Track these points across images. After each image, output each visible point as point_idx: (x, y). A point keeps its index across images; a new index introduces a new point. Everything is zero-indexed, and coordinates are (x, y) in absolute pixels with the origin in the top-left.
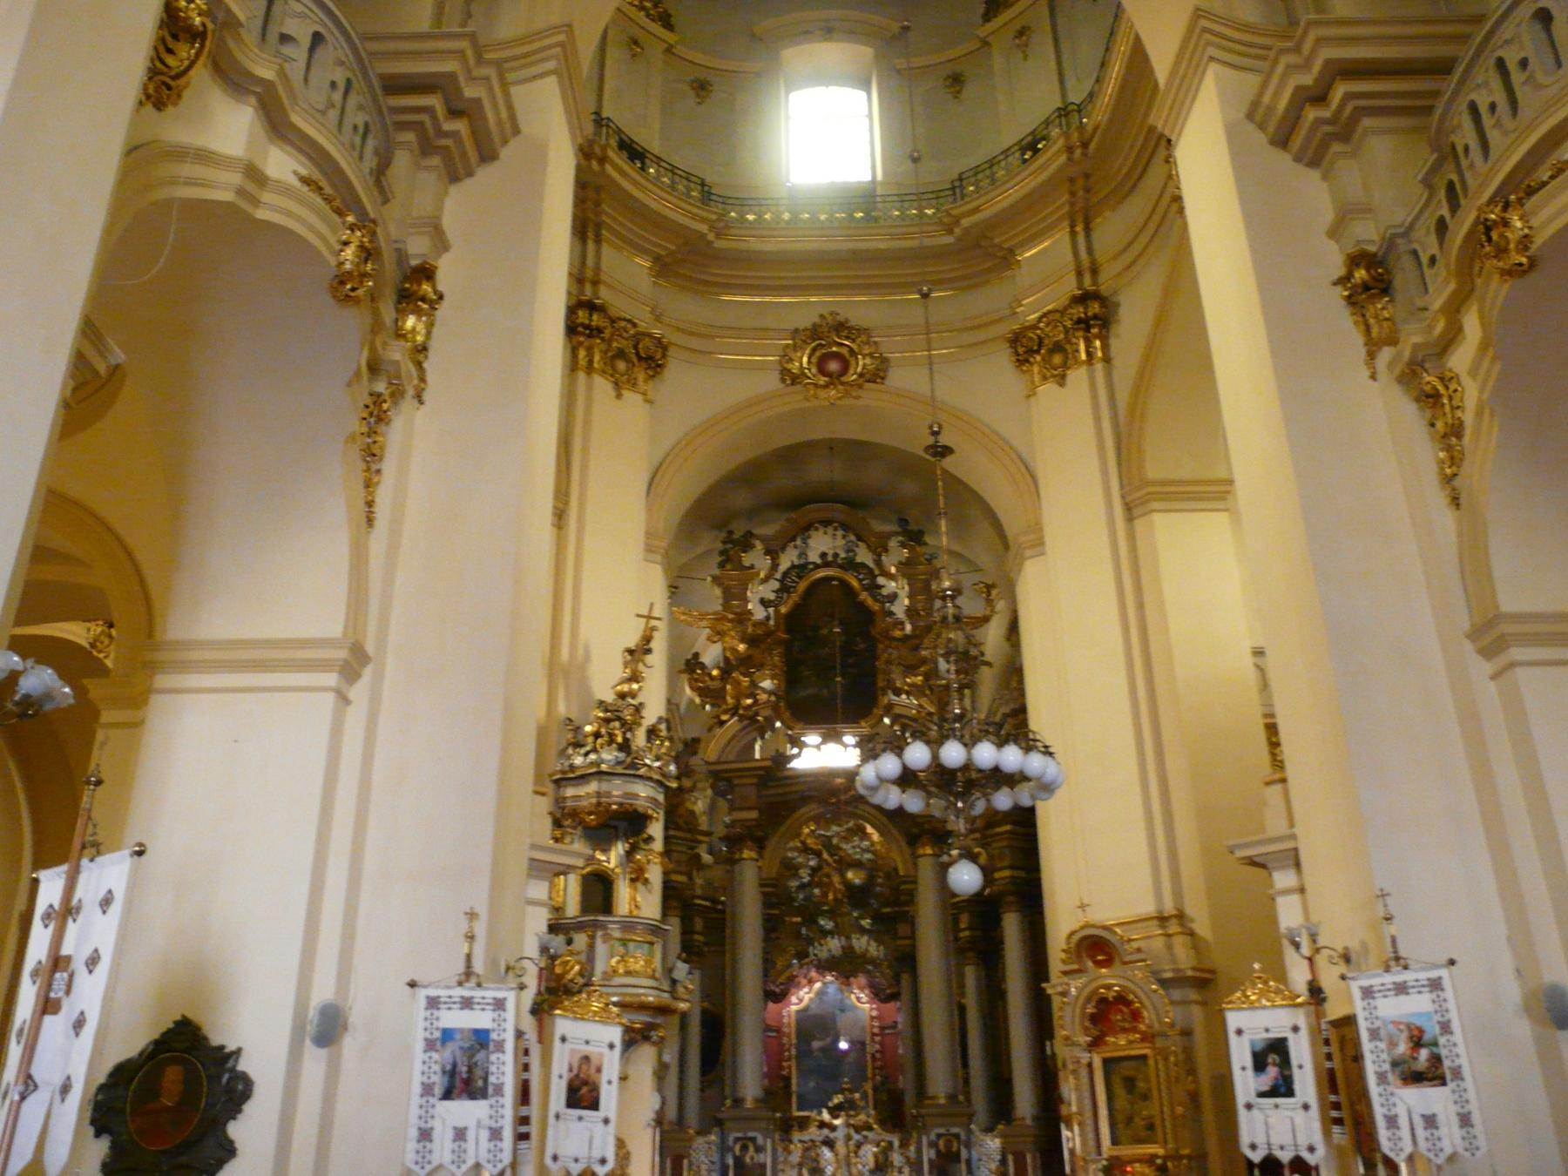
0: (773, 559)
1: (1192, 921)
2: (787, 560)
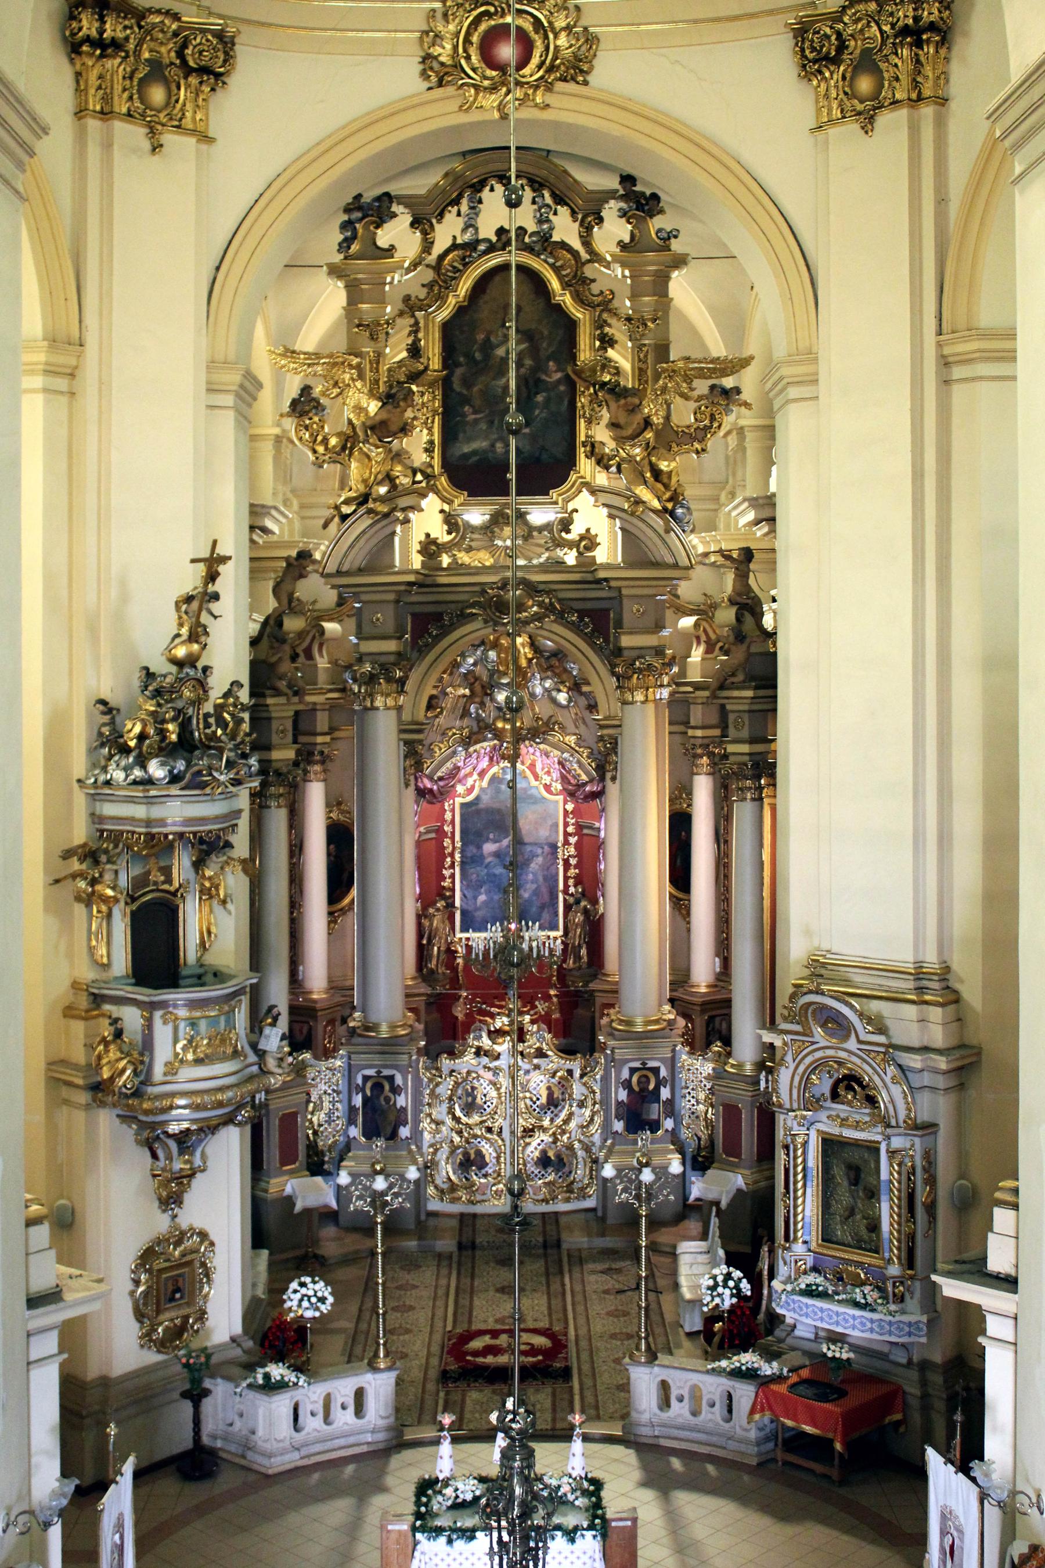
0: (425, 233)
1: (962, 981)
2: (448, 231)
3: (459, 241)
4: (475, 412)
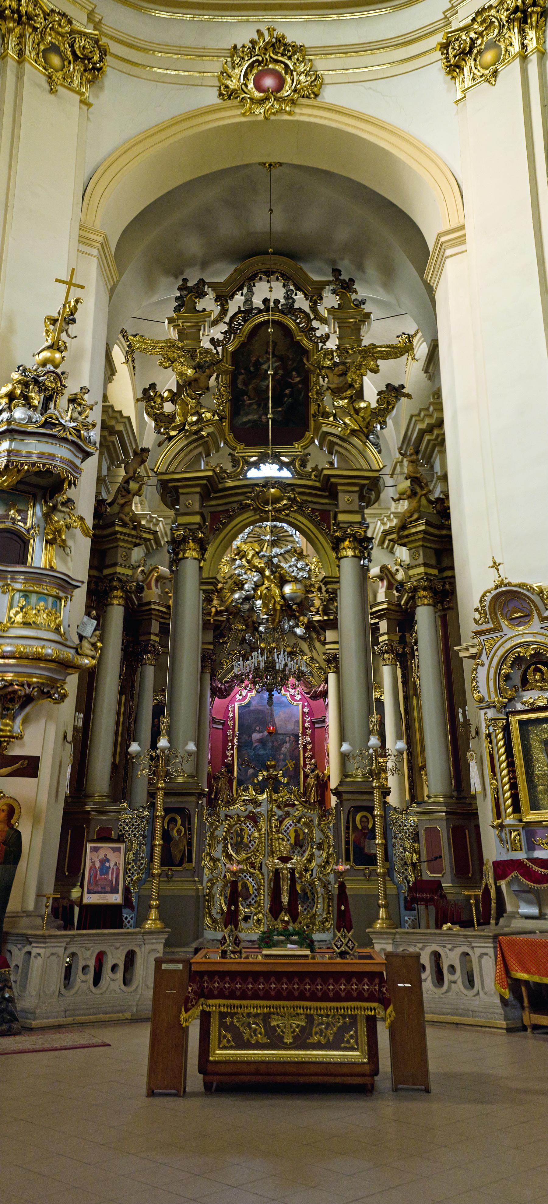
3: (242, 309)
4: (250, 399)
